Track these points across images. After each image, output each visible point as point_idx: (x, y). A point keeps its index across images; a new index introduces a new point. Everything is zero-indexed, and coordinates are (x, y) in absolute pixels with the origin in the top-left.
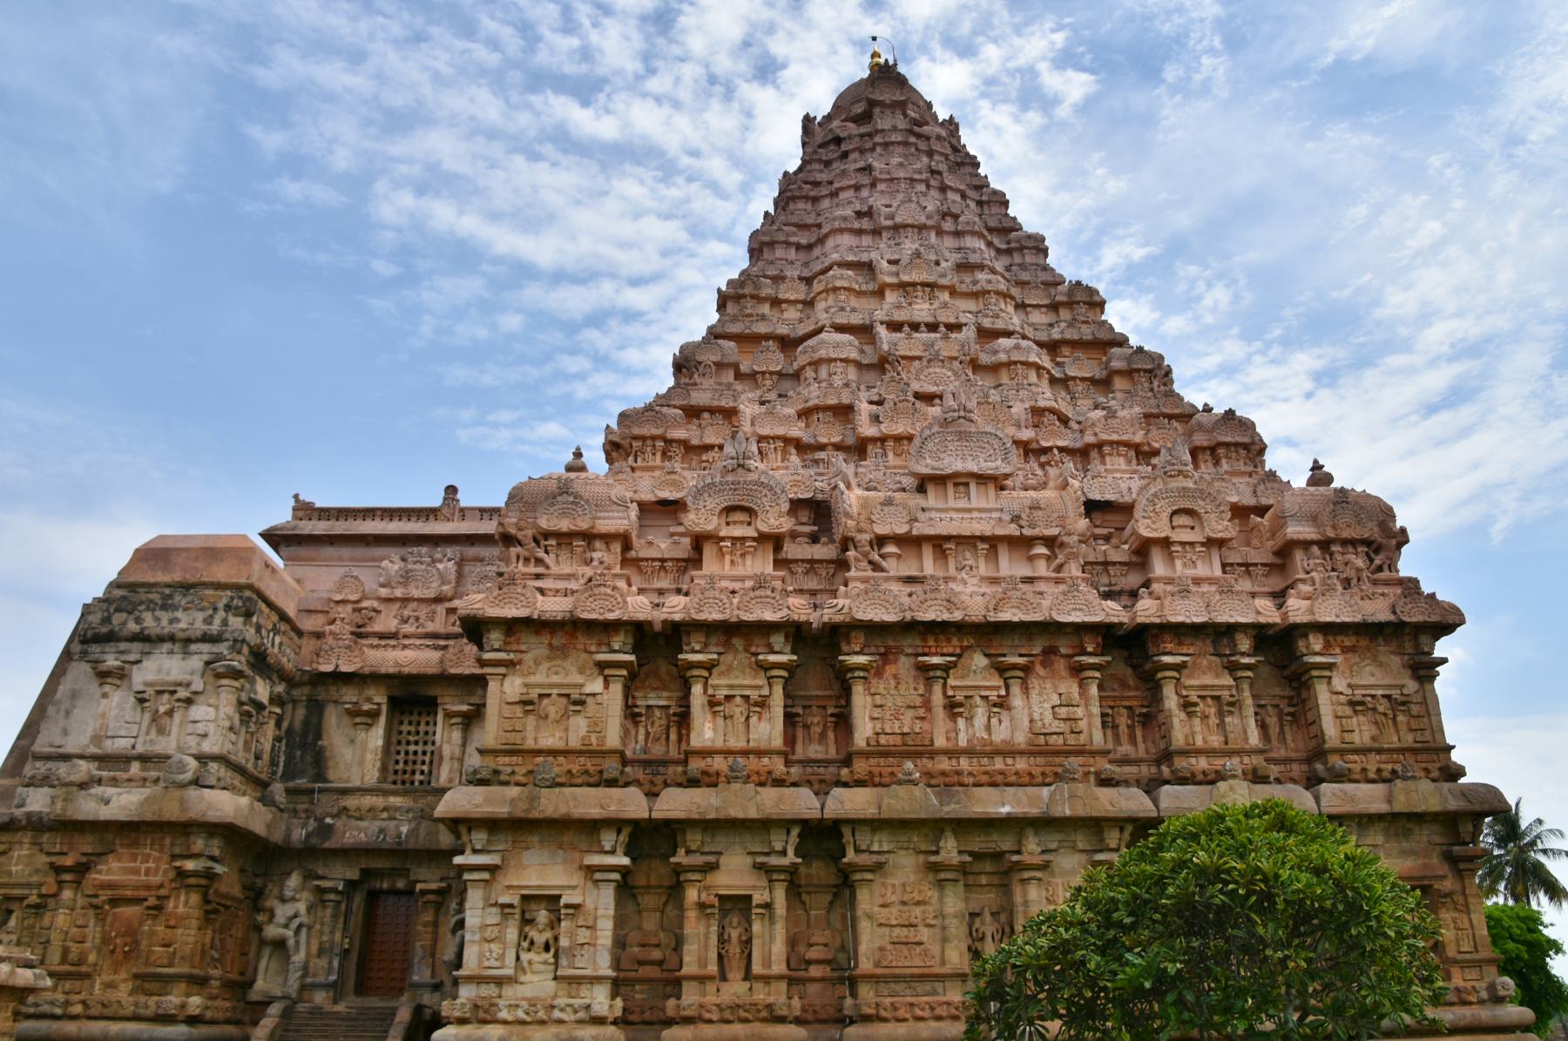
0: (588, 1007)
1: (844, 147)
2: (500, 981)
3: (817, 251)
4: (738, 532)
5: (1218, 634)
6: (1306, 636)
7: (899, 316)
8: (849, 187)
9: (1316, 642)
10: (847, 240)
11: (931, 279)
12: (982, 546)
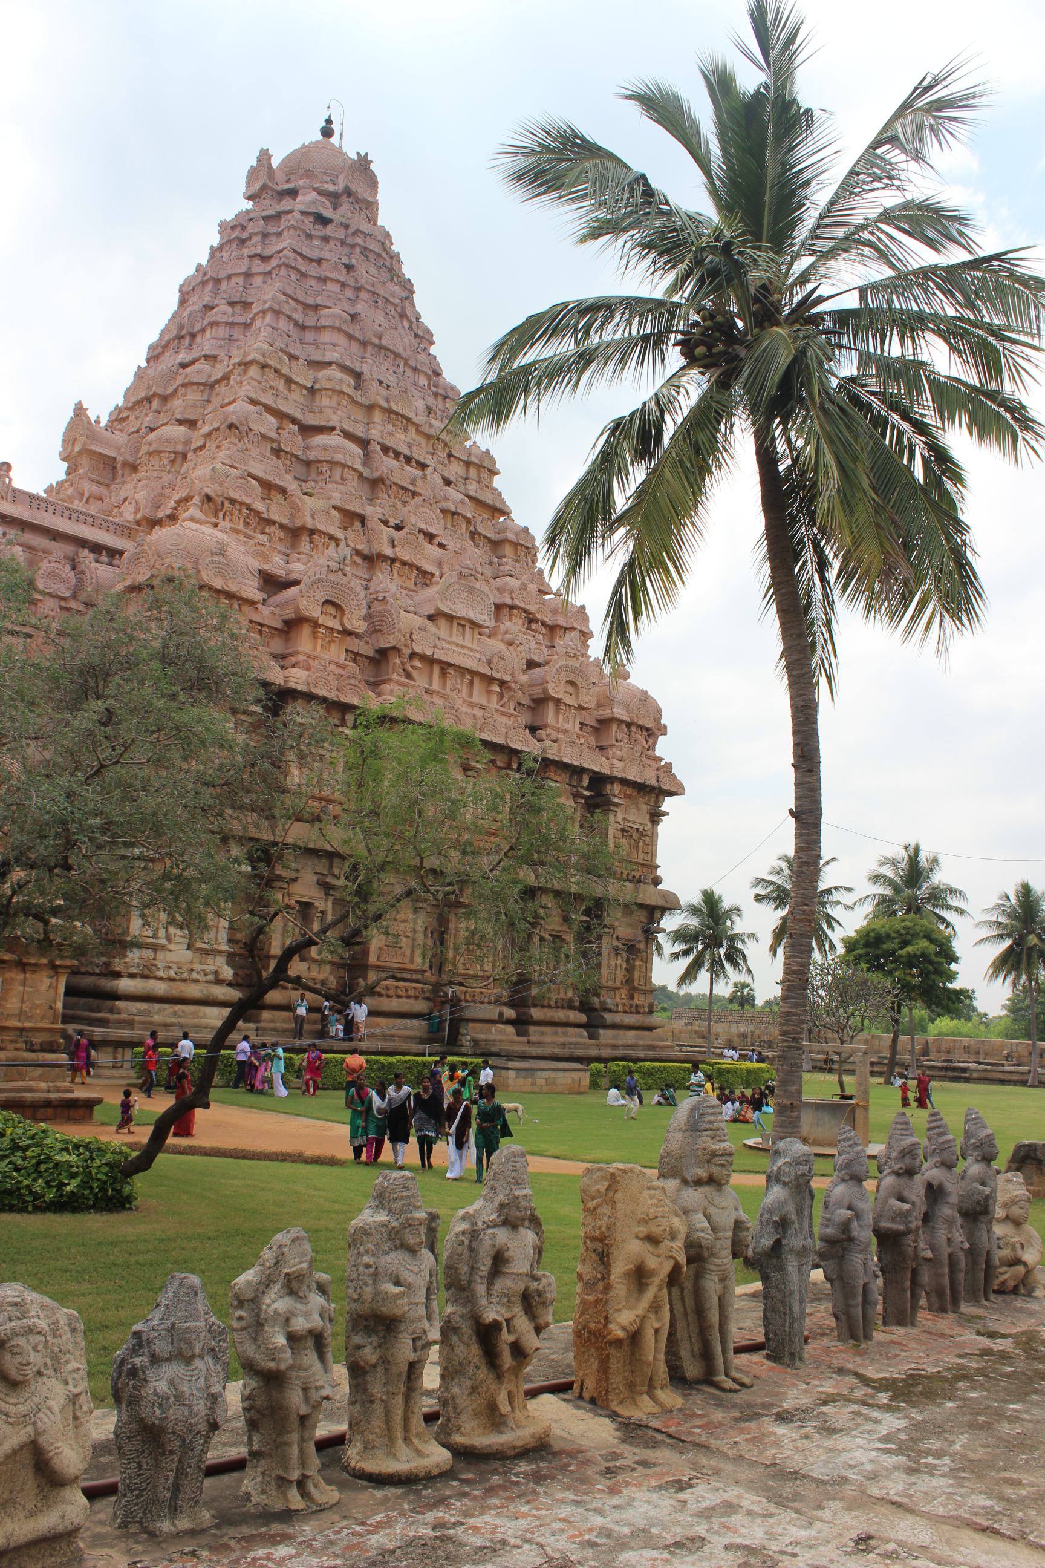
0: (216, 973)
1: (329, 230)
2: (155, 948)
3: (309, 336)
4: (330, 623)
5: (577, 771)
6: (612, 783)
7: (389, 442)
8: (338, 281)
9: (617, 788)
10: (342, 340)
11: (411, 415)
12: (468, 677)
